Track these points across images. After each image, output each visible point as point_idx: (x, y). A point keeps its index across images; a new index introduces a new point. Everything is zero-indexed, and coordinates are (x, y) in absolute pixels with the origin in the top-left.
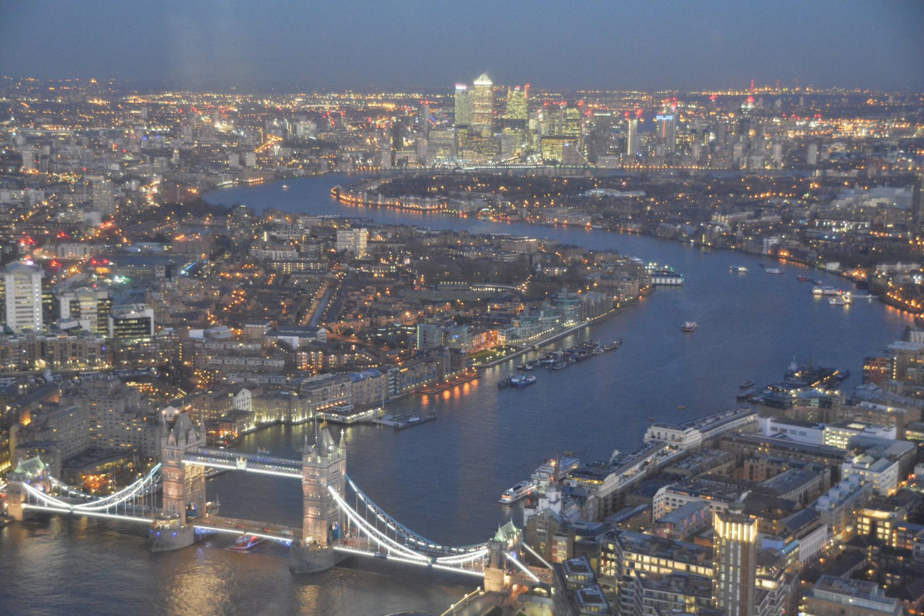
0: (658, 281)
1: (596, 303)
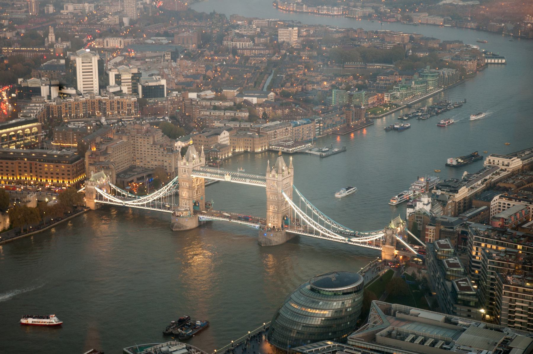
0: (489, 61)
1: (448, 76)
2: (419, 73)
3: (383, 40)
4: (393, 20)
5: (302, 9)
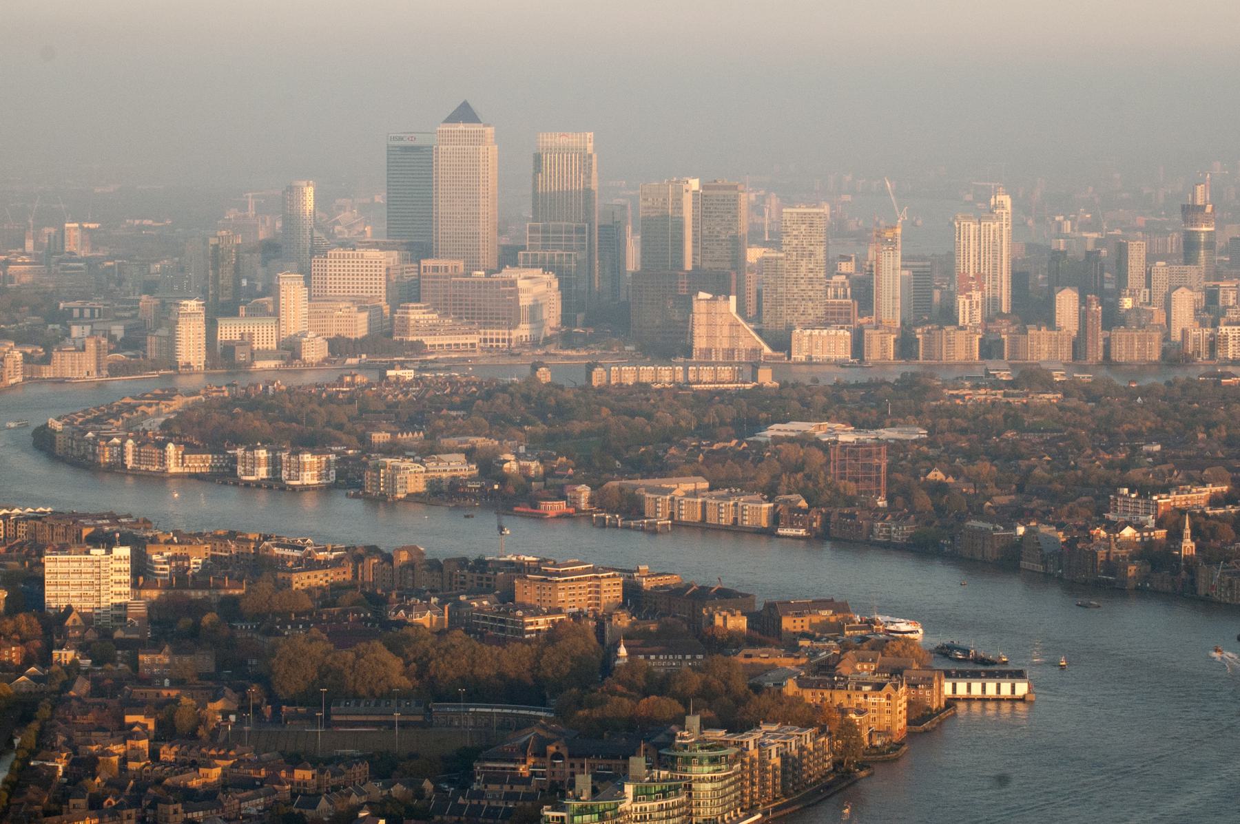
0: (962, 689)
2: (659, 746)
3: (508, 596)
4: (555, 507)
5: (163, 460)
